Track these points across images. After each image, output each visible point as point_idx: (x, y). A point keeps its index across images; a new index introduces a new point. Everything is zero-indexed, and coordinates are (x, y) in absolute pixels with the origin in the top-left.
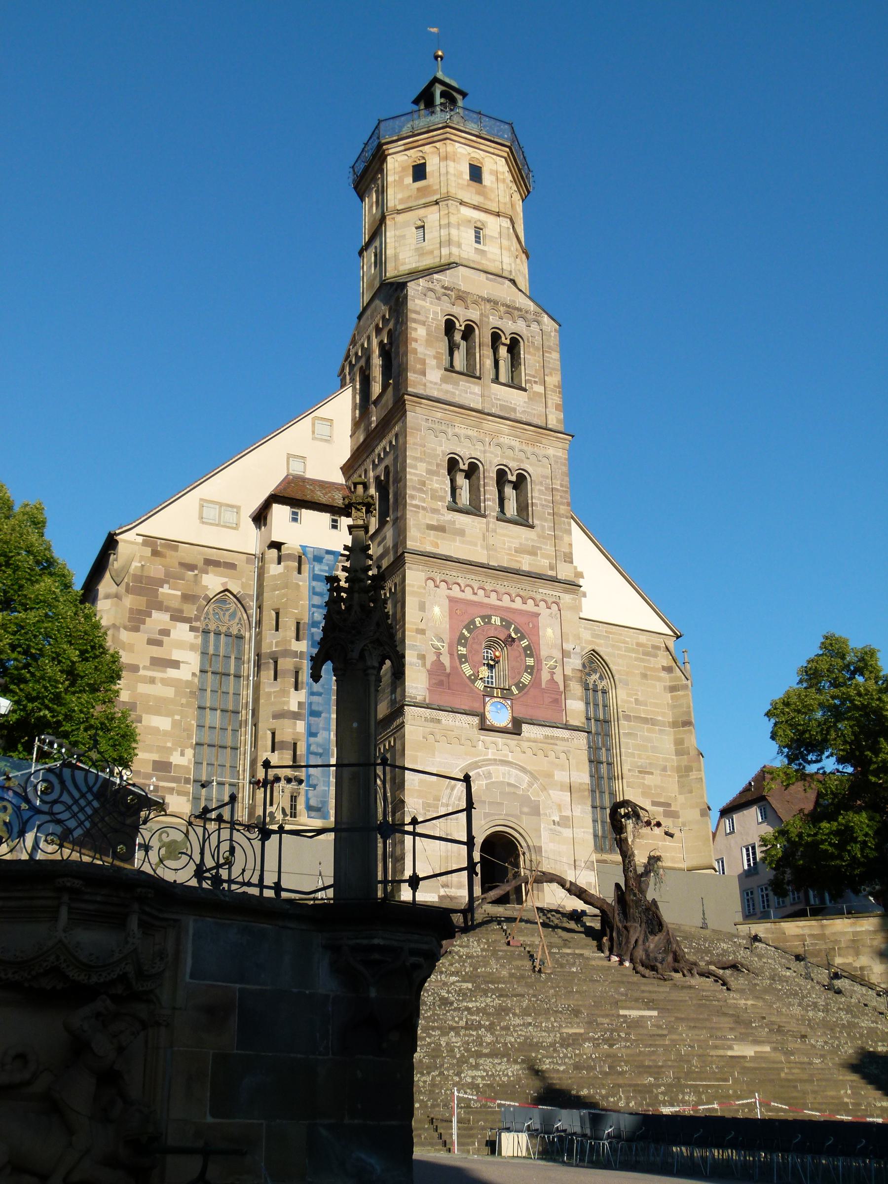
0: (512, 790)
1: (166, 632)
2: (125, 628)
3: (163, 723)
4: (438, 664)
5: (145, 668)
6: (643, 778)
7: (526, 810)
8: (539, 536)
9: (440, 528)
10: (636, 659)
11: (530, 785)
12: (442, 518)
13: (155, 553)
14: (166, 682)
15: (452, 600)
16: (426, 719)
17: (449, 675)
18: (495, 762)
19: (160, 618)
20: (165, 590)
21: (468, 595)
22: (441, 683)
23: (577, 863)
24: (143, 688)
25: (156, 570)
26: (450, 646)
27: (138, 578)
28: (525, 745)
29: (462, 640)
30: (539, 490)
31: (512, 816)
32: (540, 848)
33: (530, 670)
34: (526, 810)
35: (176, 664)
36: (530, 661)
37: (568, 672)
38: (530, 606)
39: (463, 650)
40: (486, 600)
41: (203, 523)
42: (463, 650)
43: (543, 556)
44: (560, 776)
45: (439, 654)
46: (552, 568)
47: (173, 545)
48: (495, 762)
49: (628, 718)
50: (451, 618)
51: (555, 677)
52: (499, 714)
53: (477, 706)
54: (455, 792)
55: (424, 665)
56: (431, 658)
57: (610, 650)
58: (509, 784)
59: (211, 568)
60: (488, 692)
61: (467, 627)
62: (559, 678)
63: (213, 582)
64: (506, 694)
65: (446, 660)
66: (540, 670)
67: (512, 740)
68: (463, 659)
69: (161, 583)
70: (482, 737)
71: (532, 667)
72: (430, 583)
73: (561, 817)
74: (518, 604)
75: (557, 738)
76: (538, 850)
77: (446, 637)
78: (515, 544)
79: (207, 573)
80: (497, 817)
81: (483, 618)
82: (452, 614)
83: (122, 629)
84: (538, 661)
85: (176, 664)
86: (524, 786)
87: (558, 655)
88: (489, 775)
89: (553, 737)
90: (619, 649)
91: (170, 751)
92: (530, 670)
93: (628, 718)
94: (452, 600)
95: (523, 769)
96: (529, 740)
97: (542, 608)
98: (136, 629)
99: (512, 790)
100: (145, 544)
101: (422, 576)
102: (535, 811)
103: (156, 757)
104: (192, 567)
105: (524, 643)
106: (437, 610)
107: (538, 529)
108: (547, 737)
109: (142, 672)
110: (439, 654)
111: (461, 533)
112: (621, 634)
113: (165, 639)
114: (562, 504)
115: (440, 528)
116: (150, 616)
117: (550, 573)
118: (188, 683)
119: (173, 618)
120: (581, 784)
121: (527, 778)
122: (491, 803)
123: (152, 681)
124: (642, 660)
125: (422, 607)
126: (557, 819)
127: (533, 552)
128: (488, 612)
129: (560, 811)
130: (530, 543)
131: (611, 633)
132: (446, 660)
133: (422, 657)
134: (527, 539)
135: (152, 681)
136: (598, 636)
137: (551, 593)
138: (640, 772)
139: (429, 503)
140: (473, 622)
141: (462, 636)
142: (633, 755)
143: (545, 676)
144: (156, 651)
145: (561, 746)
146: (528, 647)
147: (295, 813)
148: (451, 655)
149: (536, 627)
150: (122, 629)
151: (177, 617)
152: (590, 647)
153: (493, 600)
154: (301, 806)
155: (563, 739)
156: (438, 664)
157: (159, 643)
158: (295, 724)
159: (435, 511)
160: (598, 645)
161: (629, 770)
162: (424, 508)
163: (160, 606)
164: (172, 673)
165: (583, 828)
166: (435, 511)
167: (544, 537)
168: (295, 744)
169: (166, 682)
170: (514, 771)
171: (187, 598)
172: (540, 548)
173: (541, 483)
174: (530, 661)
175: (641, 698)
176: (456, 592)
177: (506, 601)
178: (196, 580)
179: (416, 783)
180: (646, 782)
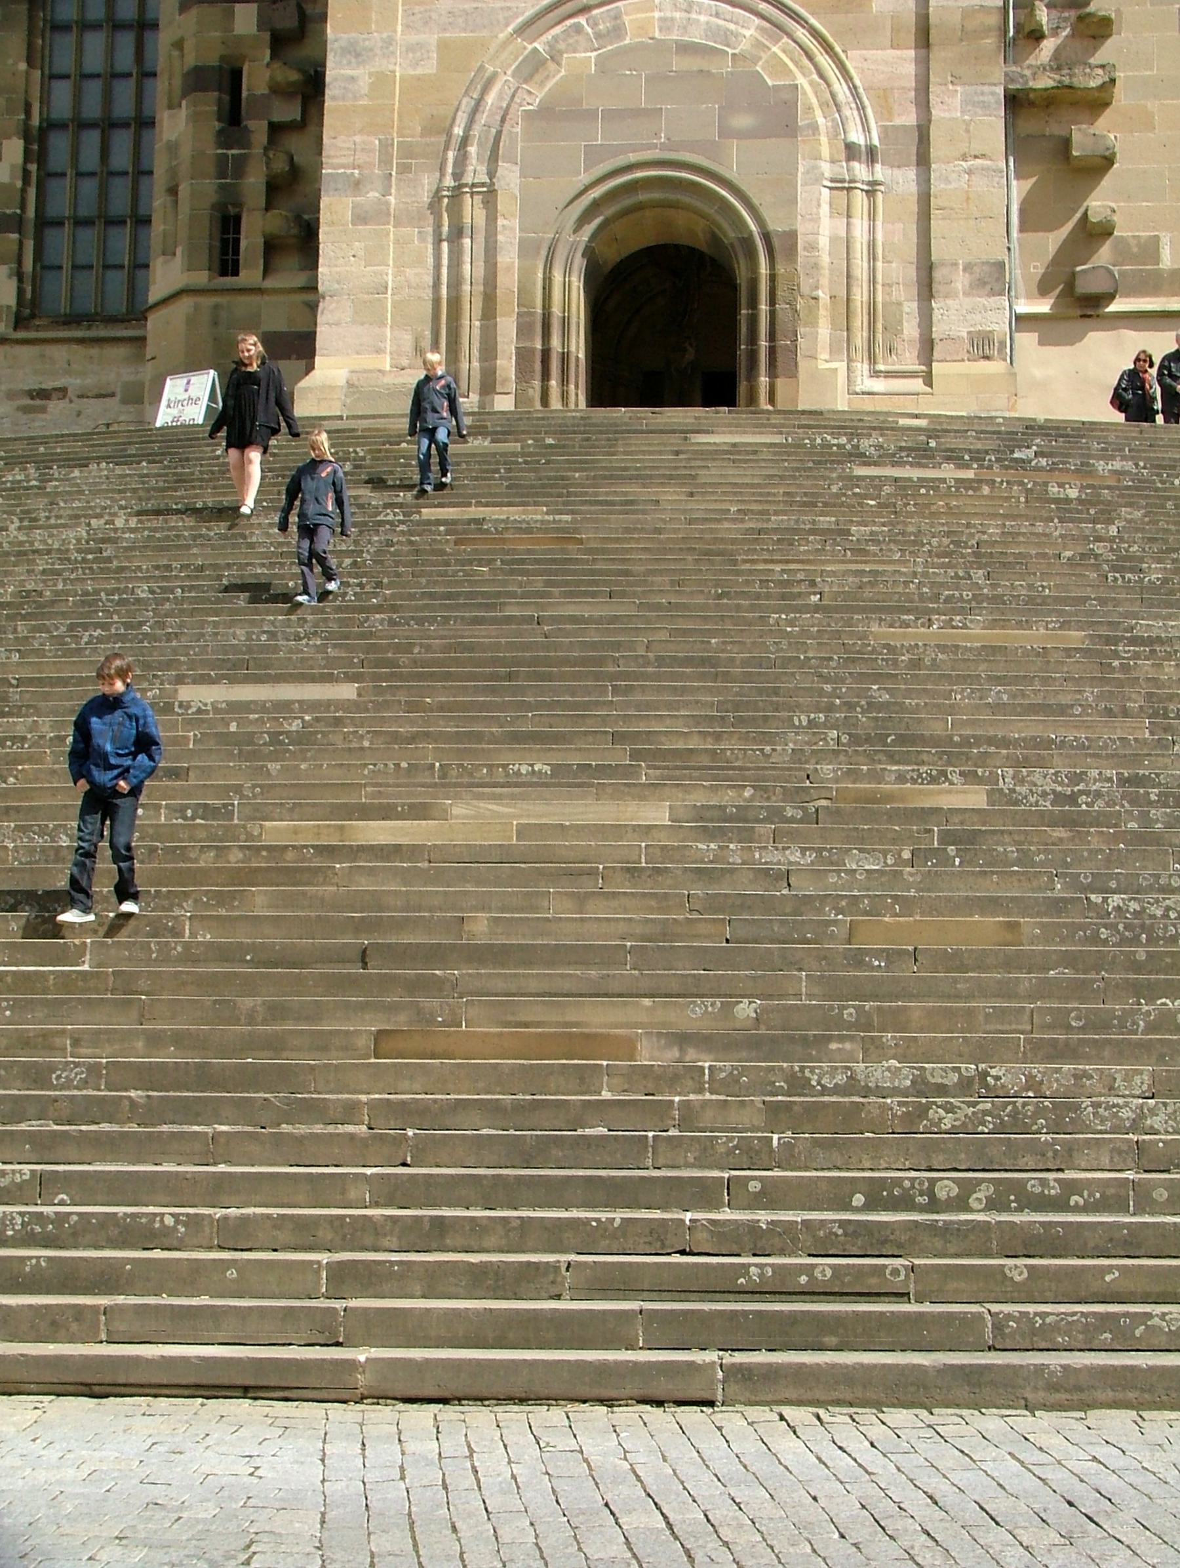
7: (743, 121)
23: (938, 275)
31: (692, 146)
32: (792, 235)
34: (743, 121)
54: (490, 99)
58: (685, 48)
76: (781, 246)
80: (633, 158)
88: (618, 31)
102: (781, 118)
120: (968, 13)
122: (611, 116)
129: (885, 110)
147: (236, 263)
154: (250, 240)
158: (231, 15)
165: (964, 158)
168: (236, 76)
179: (364, 84)
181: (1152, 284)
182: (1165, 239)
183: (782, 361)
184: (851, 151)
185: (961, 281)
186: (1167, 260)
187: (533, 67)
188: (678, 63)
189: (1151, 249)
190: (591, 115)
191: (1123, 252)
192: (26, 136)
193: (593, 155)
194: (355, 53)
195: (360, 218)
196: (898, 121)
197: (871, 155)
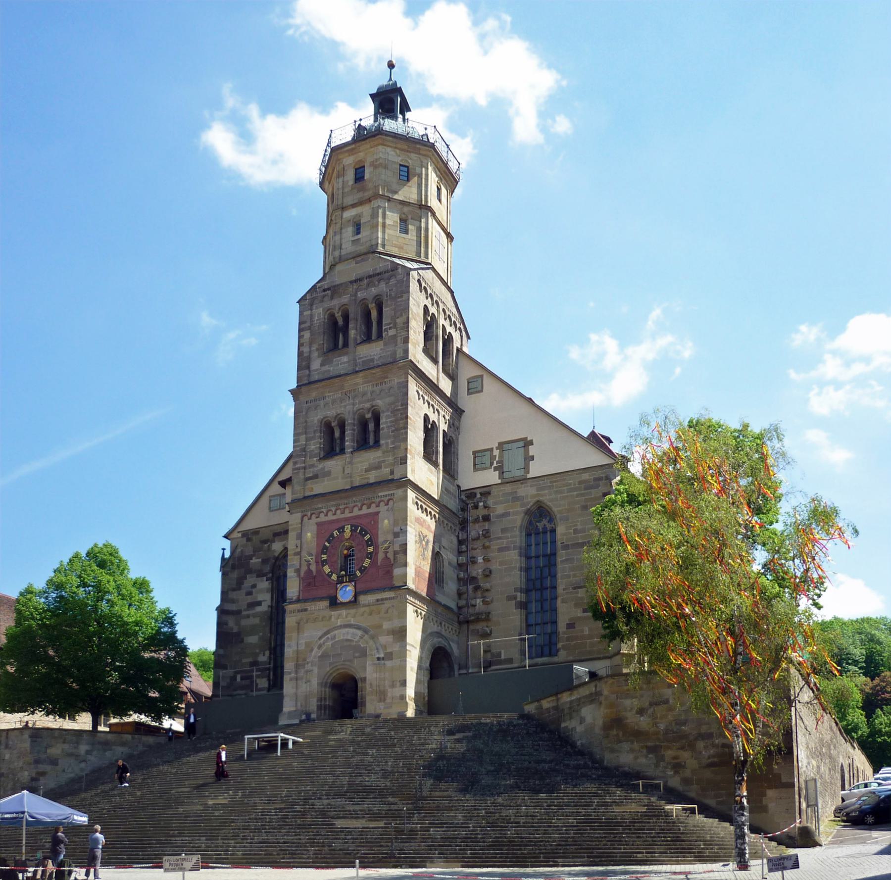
0: (348, 643)
1: (254, 586)
2: (234, 590)
3: (253, 639)
4: (309, 571)
5: (245, 610)
6: (577, 593)
7: (357, 655)
8: (384, 453)
9: (316, 477)
10: (577, 496)
11: (361, 637)
12: (316, 469)
13: (248, 540)
14: (254, 616)
15: (318, 524)
16: (299, 611)
17: (315, 577)
18: (341, 627)
19: (250, 580)
20: (254, 560)
21: (331, 517)
22: (309, 584)
24: (244, 622)
25: (249, 551)
26: (316, 558)
27: (240, 558)
28: (362, 610)
29: (324, 550)
30: (388, 417)
32: (365, 678)
33: (370, 556)
34: (357, 655)
35: (259, 603)
36: (370, 549)
37: (397, 548)
38: (373, 509)
39: (325, 557)
40: (342, 516)
41: (271, 511)
42: (325, 557)
43: (385, 468)
44: (386, 625)
45: (309, 565)
46: (392, 473)
47: (256, 532)
48: (341, 627)
49: (566, 547)
50: (317, 538)
51: (388, 555)
52: (346, 593)
53: (332, 592)
55: (299, 576)
56: (304, 568)
57: (554, 496)
58: (347, 640)
59: (276, 539)
60: (340, 581)
61: (328, 538)
62: (390, 555)
63: (277, 547)
64: (352, 578)
65: (313, 568)
66: (377, 553)
67: (352, 611)
68: (324, 563)
69: (251, 557)
70: (333, 613)
71: (371, 553)
72: (306, 519)
73: (386, 654)
74: (365, 511)
75: (386, 599)
77: (314, 552)
78: (366, 465)
79: (274, 542)
81: (338, 530)
82: (319, 535)
83: (230, 592)
84: (376, 548)
85: (259, 603)
86: (358, 638)
87: (390, 537)
89: (382, 600)
90: (561, 492)
91: (257, 655)
92: (370, 556)
93: (566, 547)
94: (318, 524)
95: (358, 628)
96: (365, 606)
97: (383, 508)
98: (239, 589)
99: (348, 643)
100: (243, 536)
101: (299, 515)
102: (364, 654)
103: (250, 660)
104: (265, 542)
105: (368, 536)
106: (309, 534)
107: (384, 447)
108: (378, 600)
109: (244, 613)
110: (309, 565)
111: (329, 473)
112: (564, 480)
113: (254, 590)
114: (402, 419)
115: (316, 477)
116: (246, 578)
117: (390, 477)
118: (265, 612)
119: (258, 576)
121: (360, 633)
123: (248, 616)
124: (582, 495)
125: (300, 537)
126: (382, 655)
127: (378, 467)
128: (340, 525)
130: (377, 460)
131: (555, 482)
132: (313, 568)
133: (298, 571)
134: (374, 459)
135: (248, 616)
136: (542, 489)
137: (387, 493)
138: (574, 588)
139: (310, 462)
140: (332, 535)
141: (325, 547)
142: (569, 576)
143: (381, 556)
144: (250, 599)
145: (387, 604)
146: (370, 539)
148: (317, 562)
149: (376, 523)
150: (230, 592)
151: (260, 574)
152: (535, 500)
153: (347, 514)
155: (390, 599)
156: (309, 571)
157: (249, 593)
159: (313, 466)
160: (542, 495)
161: (564, 589)
162: (305, 468)
163: (250, 571)
164: (259, 609)
166: (313, 466)
167: (388, 452)
169: (254, 616)
170: (351, 630)
171: (265, 561)
172: (384, 461)
173: (388, 410)
174: (370, 549)
175: (579, 527)
176: (323, 518)
177: (356, 512)
178: (269, 548)
180: (579, 595)
181: (500, 662)
182: (503, 652)
183: (364, 704)
184: (379, 659)
185: (398, 684)
186: (503, 657)
187: (320, 647)
188: (345, 644)
189: (499, 654)
190: (329, 656)
191: (493, 655)
192: (270, 649)
193: (330, 664)
194: (289, 646)
195: (291, 680)
196: (388, 651)
197: (383, 659)
